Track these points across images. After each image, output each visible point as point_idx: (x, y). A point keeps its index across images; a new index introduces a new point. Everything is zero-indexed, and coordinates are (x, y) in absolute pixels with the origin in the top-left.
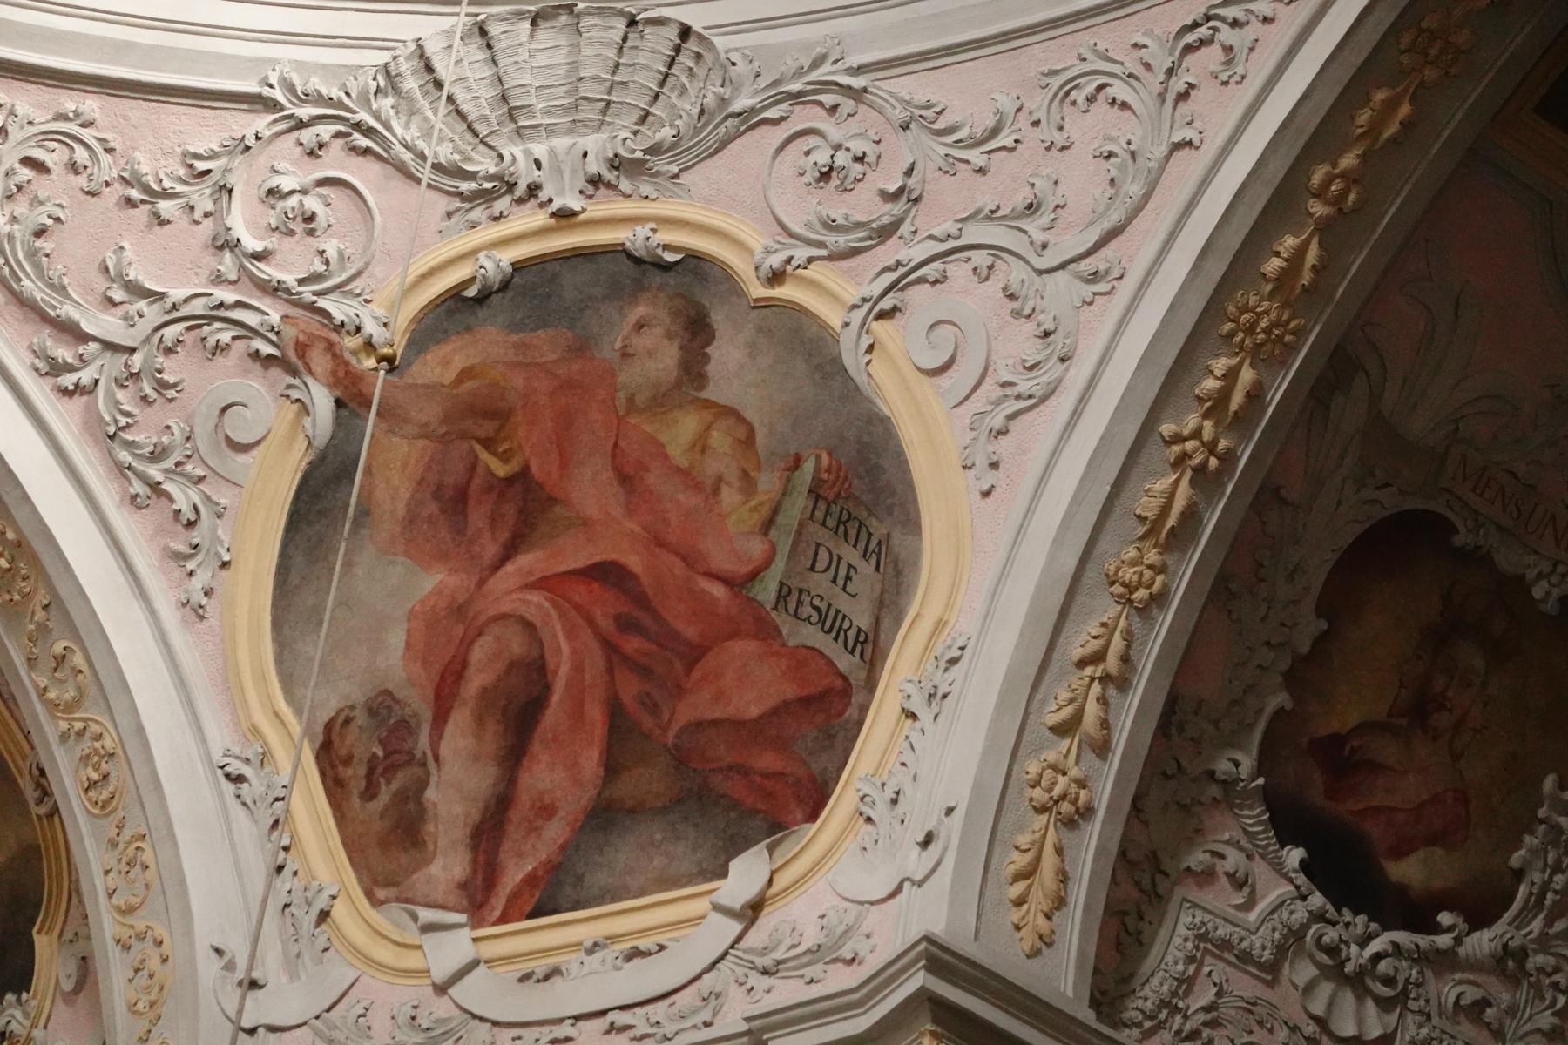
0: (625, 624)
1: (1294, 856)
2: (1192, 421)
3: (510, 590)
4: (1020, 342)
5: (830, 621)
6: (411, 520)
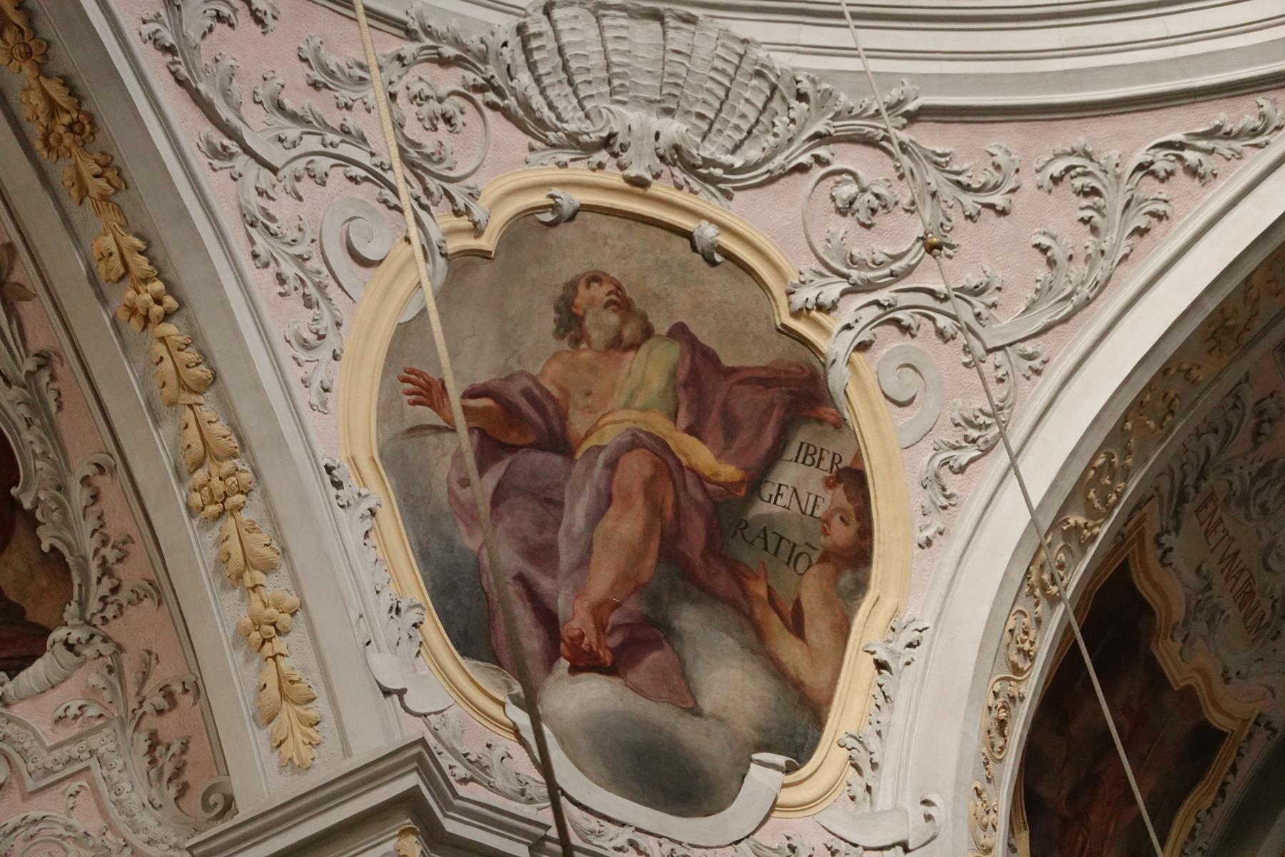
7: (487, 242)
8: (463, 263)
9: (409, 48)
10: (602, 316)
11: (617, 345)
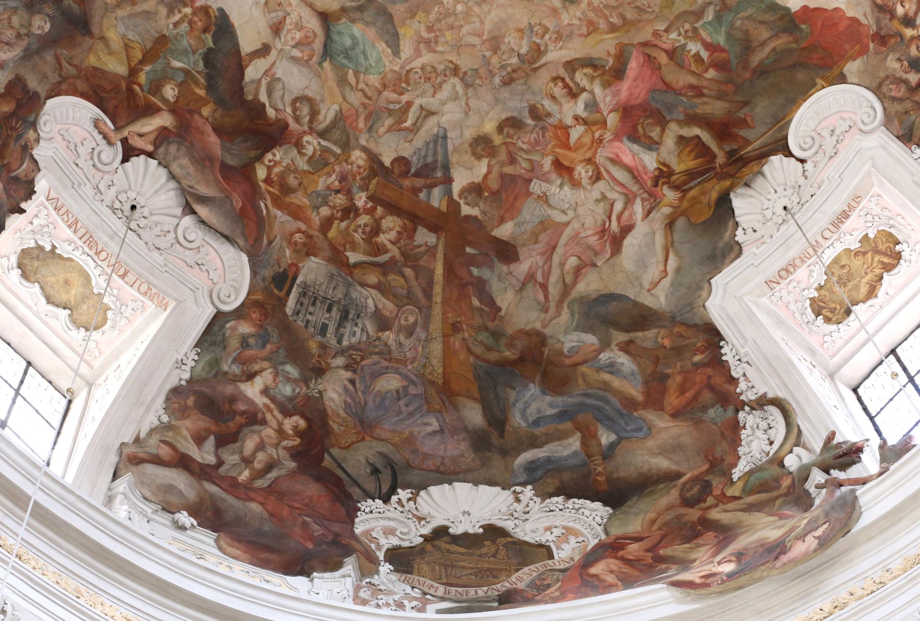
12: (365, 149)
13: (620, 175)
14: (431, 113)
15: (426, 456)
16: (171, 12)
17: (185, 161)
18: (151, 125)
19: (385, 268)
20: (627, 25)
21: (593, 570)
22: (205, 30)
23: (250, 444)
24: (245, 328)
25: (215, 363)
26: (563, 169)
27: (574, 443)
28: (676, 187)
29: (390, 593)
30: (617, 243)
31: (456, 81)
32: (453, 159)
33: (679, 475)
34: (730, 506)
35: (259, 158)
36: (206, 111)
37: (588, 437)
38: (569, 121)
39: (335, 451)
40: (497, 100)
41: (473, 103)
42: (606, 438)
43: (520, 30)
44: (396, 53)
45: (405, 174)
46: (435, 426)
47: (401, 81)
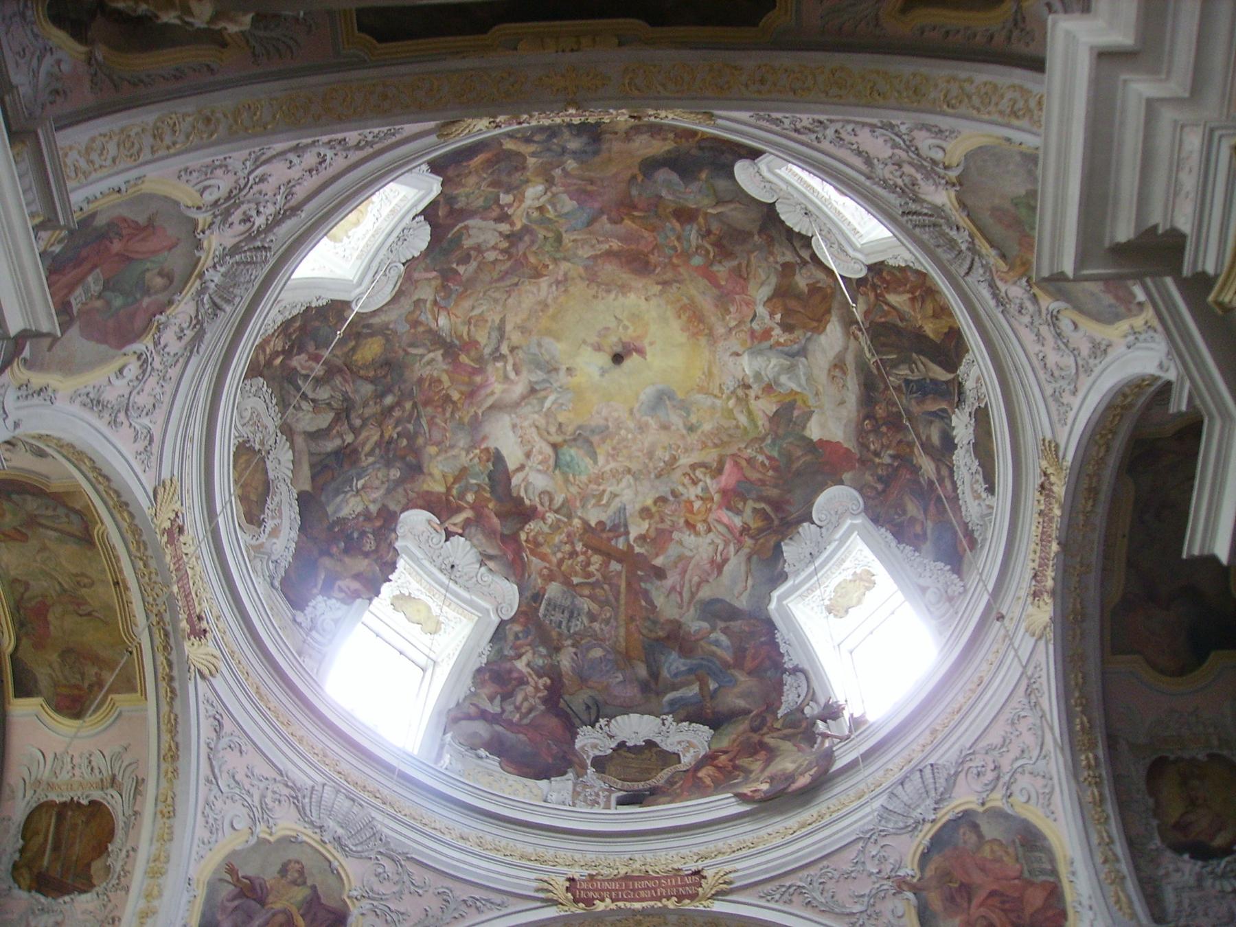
0: (1003, 902)
1: (1186, 856)
2: (1086, 774)
3: (976, 911)
4: (1040, 782)
5: (1043, 872)
6: (945, 909)
7: (272, 839)
8: (262, 842)
9: (279, 778)
10: (292, 872)
11: (294, 883)
12: (580, 518)
13: (721, 528)
14: (616, 496)
15: (616, 697)
16: (468, 453)
17: (480, 536)
18: (460, 518)
19: (593, 586)
20: (723, 444)
21: (700, 774)
22: (488, 460)
23: (519, 697)
24: (517, 628)
25: (500, 651)
26: (690, 525)
27: (695, 689)
28: (752, 537)
29: (592, 786)
30: (720, 568)
31: (629, 476)
32: (630, 521)
33: (749, 712)
34: (775, 734)
35: (522, 528)
36: (491, 505)
37: (703, 685)
38: (693, 498)
39: (566, 697)
40: (653, 486)
41: (639, 488)
42: (712, 686)
43: (665, 448)
44: (596, 462)
45: (603, 530)
46: (621, 678)
47: (599, 478)
